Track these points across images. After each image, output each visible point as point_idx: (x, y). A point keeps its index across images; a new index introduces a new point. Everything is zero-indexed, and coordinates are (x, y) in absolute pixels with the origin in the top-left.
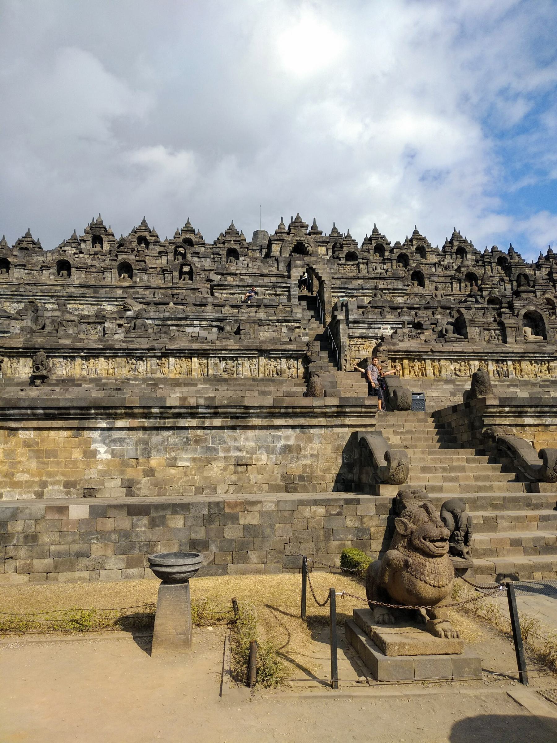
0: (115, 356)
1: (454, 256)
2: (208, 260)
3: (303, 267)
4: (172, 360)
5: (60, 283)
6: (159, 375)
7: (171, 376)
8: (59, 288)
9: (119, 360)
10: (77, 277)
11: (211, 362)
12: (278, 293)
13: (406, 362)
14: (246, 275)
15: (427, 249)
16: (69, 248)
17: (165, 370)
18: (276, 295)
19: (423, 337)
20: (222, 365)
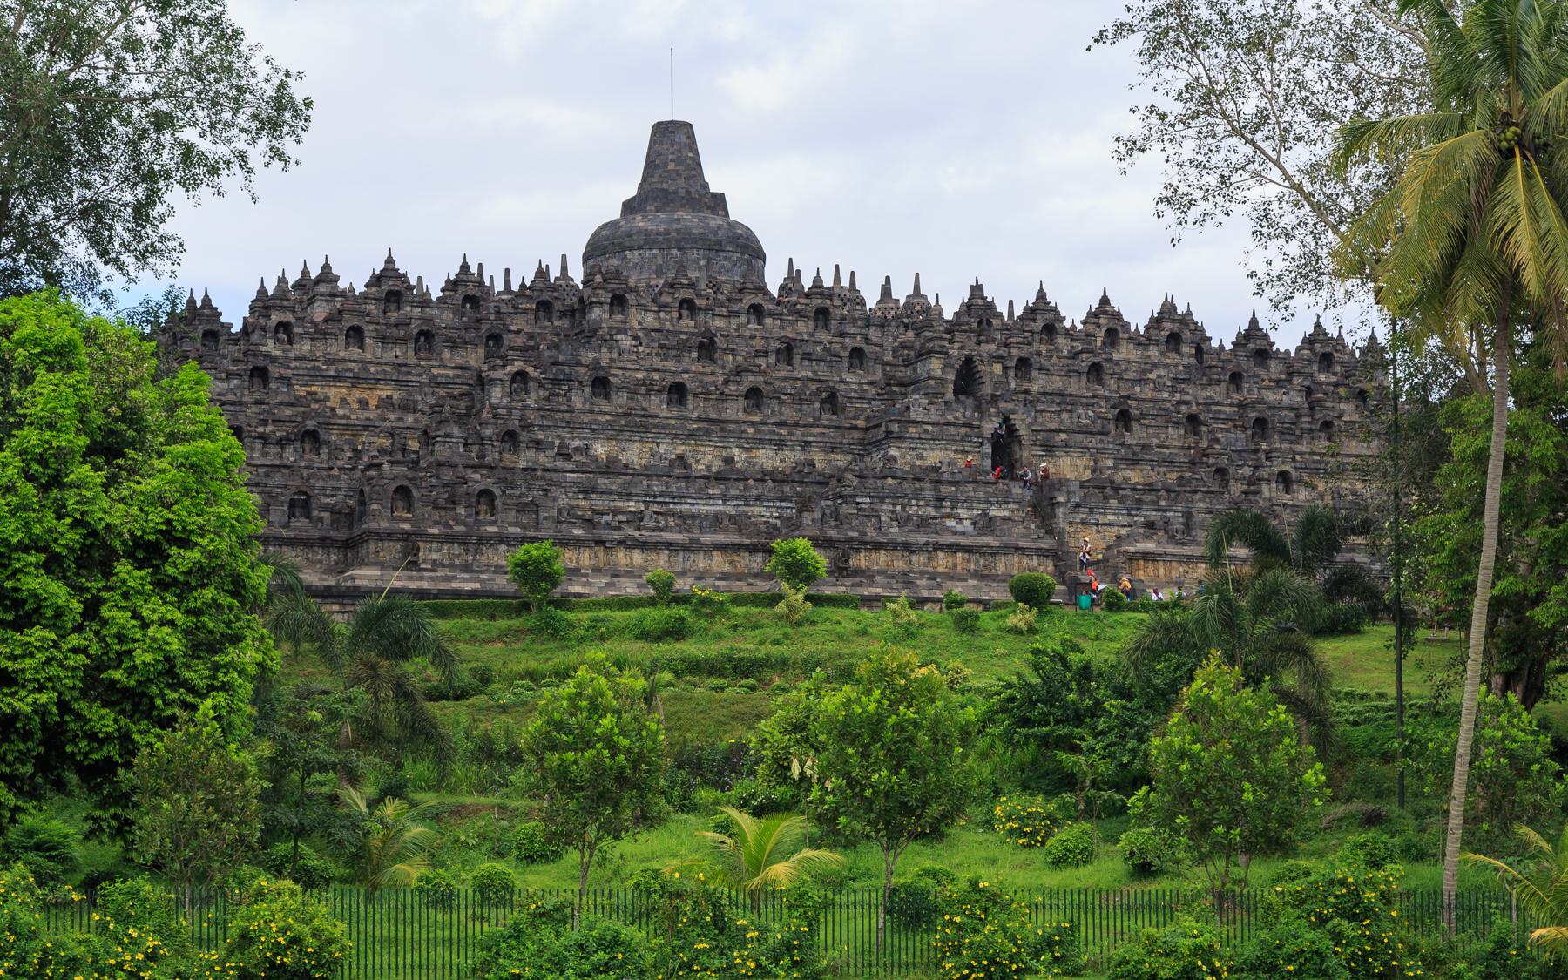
0: (895, 549)
1: (1163, 347)
2: (822, 363)
3: (997, 416)
4: (941, 554)
5: (675, 414)
6: (930, 569)
7: (940, 570)
8: (673, 422)
9: (896, 553)
10: (694, 408)
11: (973, 558)
12: (967, 449)
13: (1141, 562)
14: (928, 423)
15: (1121, 335)
16: (623, 337)
17: (935, 564)
18: (964, 452)
19: (1155, 537)
20: (982, 561)
